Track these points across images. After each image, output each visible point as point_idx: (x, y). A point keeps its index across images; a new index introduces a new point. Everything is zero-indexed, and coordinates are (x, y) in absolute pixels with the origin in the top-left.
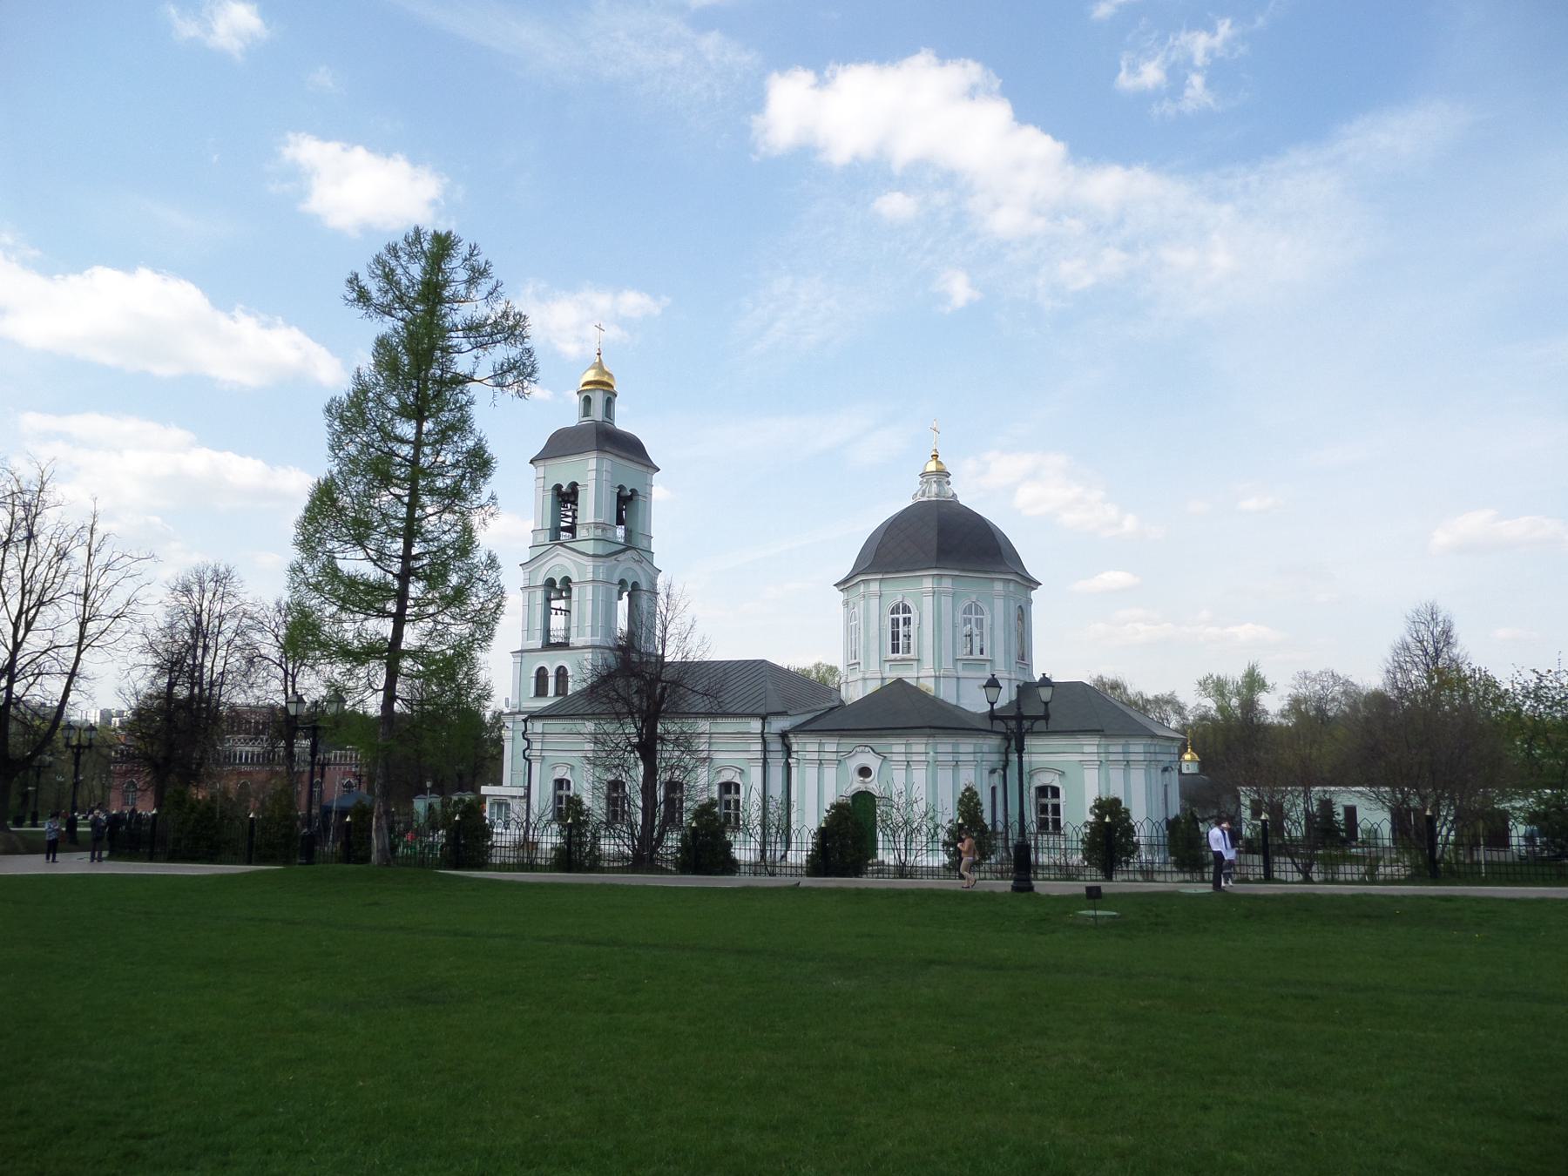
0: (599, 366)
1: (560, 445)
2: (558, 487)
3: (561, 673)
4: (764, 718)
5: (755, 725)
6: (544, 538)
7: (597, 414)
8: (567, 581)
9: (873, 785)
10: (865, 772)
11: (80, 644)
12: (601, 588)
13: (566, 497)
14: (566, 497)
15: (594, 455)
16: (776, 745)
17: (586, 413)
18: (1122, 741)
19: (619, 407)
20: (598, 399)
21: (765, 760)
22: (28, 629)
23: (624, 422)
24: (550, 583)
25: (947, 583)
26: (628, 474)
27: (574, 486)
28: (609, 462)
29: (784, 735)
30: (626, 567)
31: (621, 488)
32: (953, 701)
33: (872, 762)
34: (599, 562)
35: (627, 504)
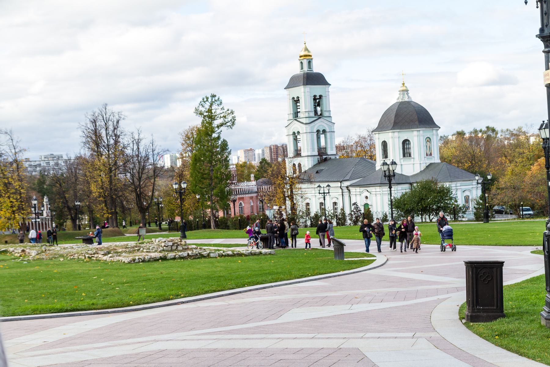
0: (306, 49)
1: (293, 83)
2: (293, 98)
3: (300, 165)
4: (341, 182)
5: (339, 184)
6: (291, 117)
7: (306, 69)
8: (299, 132)
9: (368, 202)
10: (367, 197)
11: (154, 175)
12: (309, 135)
13: (296, 101)
14: (296, 101)
15: (302, 87)
16: (346, 190)
17: (302, 68)
18: (455, 183)
19: (314, 63)
20: (305, 62)
21: (343, 195)
22: (142, 174)
23: (316, 69)
24: (294, 133)
25: (396, 134)
26: (317, 90)
27: (298, 97)
28: (309, 88)
29: (347, 187)
30: (320, 124)
31: (315, 96)
32: (400, 173)
33: (367, 194)
34: (307, 126)
35: (317, 101)
